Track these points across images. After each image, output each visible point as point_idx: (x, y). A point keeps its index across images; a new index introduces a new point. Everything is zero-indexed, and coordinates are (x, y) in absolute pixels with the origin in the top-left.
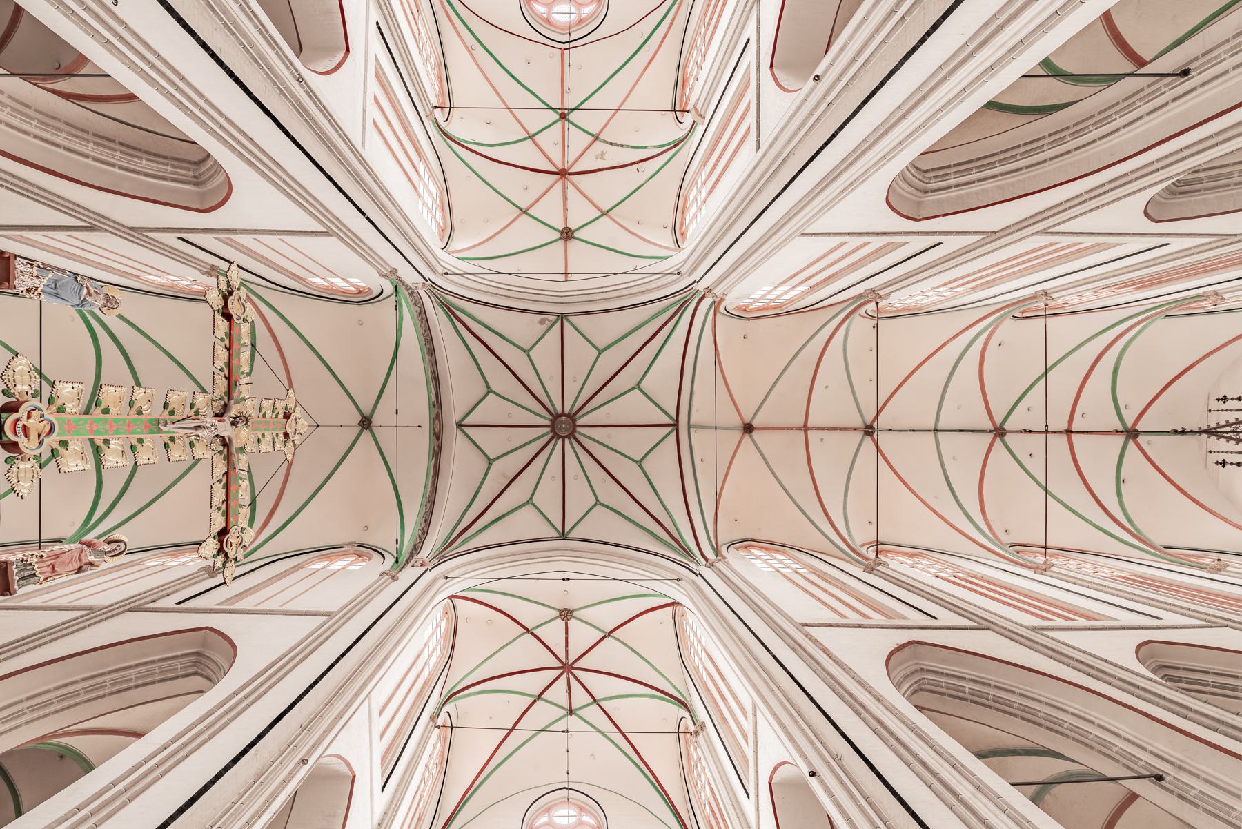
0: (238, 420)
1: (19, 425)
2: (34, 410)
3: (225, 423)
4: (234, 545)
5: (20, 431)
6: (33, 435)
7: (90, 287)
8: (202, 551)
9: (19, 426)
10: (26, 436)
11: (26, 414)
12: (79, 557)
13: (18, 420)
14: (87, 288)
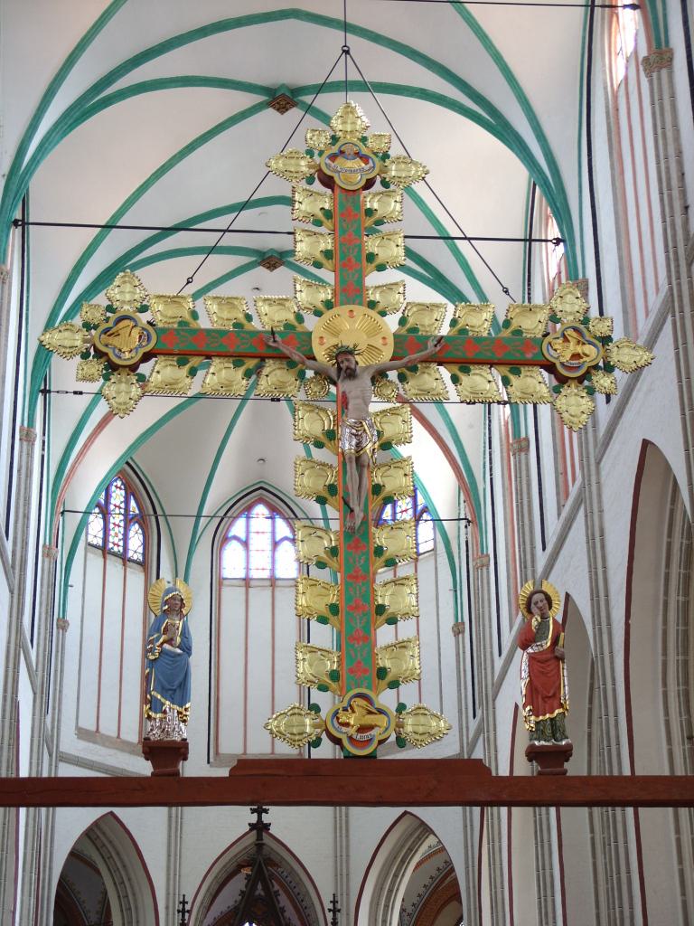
0: (343, 366)
1: (358, 737)
2: (338, 718)
3: (349, 396)
4: (579, 349)
5: (365, 736)
6: (370, 720)
7: (161, 640)
8: (575, 420)
9: (359, 737)
10: (371, 728)
11: (344, 729)
12: (542, 663)
13: (350, 738)
14: (162, 644)
